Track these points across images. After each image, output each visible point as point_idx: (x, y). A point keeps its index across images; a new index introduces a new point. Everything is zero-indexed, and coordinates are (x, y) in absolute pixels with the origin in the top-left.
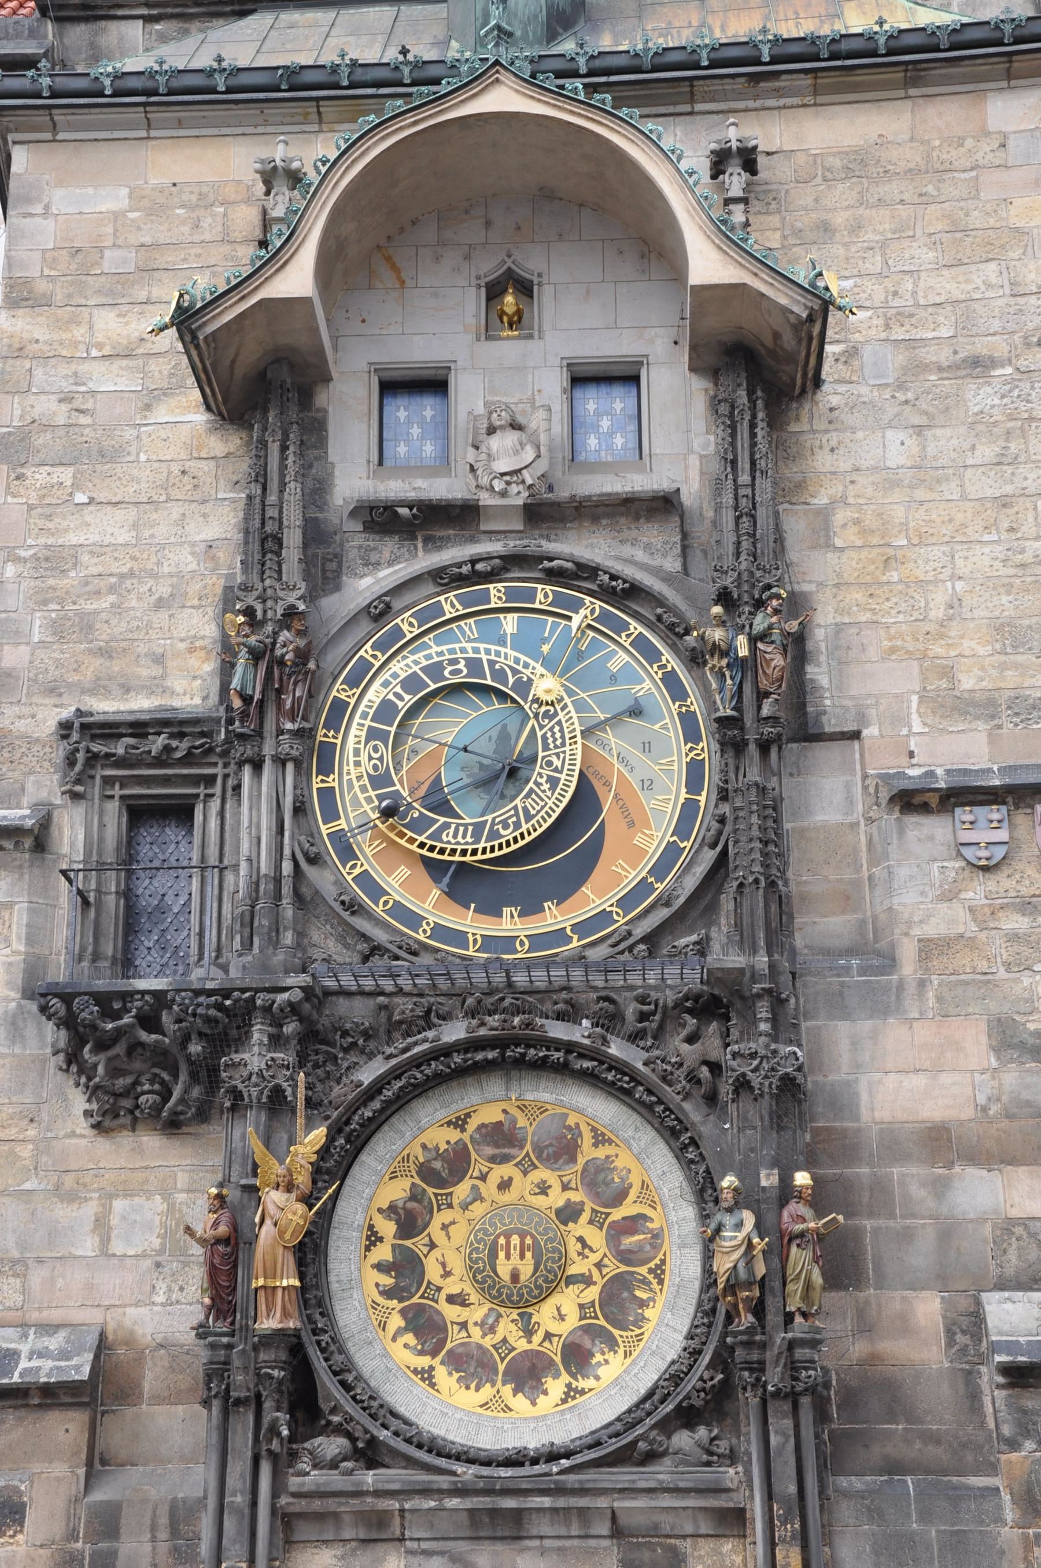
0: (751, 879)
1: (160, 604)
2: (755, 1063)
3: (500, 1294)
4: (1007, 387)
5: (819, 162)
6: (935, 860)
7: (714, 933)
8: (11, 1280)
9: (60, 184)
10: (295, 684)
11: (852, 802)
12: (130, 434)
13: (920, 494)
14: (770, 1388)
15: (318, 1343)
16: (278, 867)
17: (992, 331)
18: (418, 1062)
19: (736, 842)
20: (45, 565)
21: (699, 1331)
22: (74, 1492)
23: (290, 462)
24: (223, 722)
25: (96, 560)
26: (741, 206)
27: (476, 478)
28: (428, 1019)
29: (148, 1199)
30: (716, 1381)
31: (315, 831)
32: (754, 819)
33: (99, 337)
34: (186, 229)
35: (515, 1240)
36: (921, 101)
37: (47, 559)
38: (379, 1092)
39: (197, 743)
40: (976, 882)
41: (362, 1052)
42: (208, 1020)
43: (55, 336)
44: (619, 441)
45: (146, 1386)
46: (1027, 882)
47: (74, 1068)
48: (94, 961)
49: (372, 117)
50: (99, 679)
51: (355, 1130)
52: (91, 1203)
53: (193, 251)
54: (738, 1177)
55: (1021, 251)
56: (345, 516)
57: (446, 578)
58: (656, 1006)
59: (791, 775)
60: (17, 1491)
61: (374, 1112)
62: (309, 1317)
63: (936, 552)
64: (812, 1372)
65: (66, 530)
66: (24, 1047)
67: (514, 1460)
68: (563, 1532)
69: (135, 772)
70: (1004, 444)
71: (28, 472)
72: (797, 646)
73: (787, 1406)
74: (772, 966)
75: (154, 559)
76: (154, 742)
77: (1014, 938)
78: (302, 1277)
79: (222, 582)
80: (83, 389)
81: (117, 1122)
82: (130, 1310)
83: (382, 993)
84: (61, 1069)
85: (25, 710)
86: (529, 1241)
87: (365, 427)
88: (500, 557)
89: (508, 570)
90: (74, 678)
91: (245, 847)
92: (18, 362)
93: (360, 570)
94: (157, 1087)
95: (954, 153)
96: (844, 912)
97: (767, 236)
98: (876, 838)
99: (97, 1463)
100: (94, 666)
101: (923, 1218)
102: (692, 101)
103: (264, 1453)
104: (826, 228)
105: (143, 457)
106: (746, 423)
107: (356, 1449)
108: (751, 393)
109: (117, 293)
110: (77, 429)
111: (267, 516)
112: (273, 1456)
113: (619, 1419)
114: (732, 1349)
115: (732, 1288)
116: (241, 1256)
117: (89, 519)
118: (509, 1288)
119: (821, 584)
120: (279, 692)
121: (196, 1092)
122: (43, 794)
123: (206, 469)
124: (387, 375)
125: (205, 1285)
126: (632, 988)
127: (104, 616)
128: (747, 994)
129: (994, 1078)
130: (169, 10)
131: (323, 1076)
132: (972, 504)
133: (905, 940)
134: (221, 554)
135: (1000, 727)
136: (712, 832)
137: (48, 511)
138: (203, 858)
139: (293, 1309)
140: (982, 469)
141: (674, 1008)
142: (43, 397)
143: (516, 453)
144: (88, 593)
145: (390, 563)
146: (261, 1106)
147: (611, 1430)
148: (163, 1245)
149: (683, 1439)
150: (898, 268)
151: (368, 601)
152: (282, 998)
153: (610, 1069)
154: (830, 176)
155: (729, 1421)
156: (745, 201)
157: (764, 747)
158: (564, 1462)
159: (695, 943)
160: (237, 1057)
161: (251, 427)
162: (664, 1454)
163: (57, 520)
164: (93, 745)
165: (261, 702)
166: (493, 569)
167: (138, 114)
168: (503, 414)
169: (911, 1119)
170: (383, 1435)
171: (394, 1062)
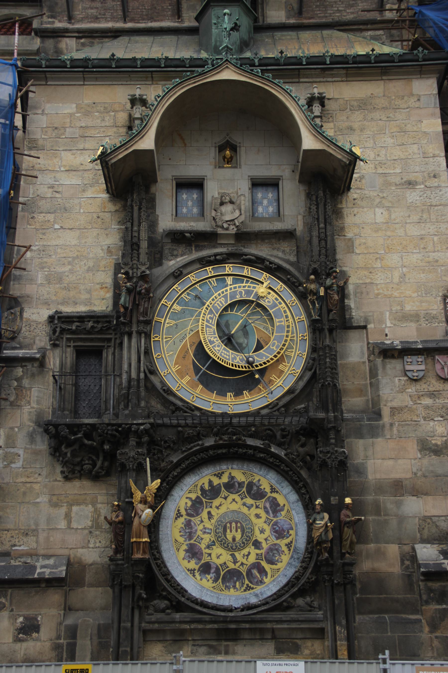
1: (89, 270)
2: (329, 455)
4: (422, 193)
5: (348, 102)
6: (396, 377)
7: (311, 404)
8: (32, 538)
9: (48, 102)
10: (145, 302)
11: (363, 353)
12: (76, 201)
14: (335, 582)
15: (157, 563)
16: (138, 375)
17: (416, 171)
19: (320, 369)
20: (42, 253)
22: (59, 621)
23: (142, 214)
25: (63, 251)
26: (319, 119)
27: (216, 222)
28: (199, 437)
29: (86, 506)
31: (152, 361)
32: (328, 360)
33: (64, 163)
34: (99, 121)
35: (234, 525)
36: (387, 81)
38: (180, 465)
41: (172, 449)
42: (113, 436)
44: (271, 209)
45: (87, 580)
46: (432, 386)
47: (57, 454)
49: (177, 80)
50: (64, 298)
52: (63, 508)
53: (102, 130)
54: (322, 500)
55: (426, 141)
57: (205, 262)
59: (339, 342)
61: (178, 473)
62: (153, 553)
64: (351, 576)
68: (253, 637)
69: (79, 336)
70: (421, 215)
72: (342, 292)
73: (342, 589)
74: (335, 417)
76: (88, 324)
77: (427, 407)
78: (150, 537)
79: (114, 261)
80: (57, 183)
82: (80, 551)
83: (180, 426)
85: (35, 311)
86: (239, 525)
87: (171, 201)
88: (226, 254)
89: (229, 259)
90: (54, 298)
91: (125, 367)
93: (170, 258)
94: (91, 462)
96: (360, 396)
97: (329, 130)
99: (68, 609)
101: (392, 516)
102: (299, 77)
104: (351, 129)
105: (82, 211)
106: (322, 204)
107: (172, 605)
108: (324, 192)
110: (55, 199)
112: (140, 608)
113: (275, 594)
115: (320, 543)
120: (138, 305)
121: (106, 464)
122: (42, 344)
123: (107, 216)
125: (113, 540)
126: (279, 425)
127: (66, 274)
130: (86, 35)
131: (157, 458)
132: (409, 238)
133: (385, 408)
134: (113, 250)
136: (310, 364)
138: (106, 371)
139: (147, 550)
140: (413, 224)
142: (42, 186)
143: (232, 213)
145: (182, 255)
146: (134, 470)
147: (271, 598)
148: (93, 524)
149: (300, 601)
150: (380, 145)
152: (142, 427)
153: (271, 457)
154: (352, 109)
156: (320, 117)
157: (331, 331)
158: (255, 611)
159: (304, 408)
160: (123, 451)
162: (293, 607)
163: (47, 235)
165: (131, 310)
166: (223, 258)
167: (81, 75)
168: (227, 197)
169: (387, 477)
170: (183, 599)
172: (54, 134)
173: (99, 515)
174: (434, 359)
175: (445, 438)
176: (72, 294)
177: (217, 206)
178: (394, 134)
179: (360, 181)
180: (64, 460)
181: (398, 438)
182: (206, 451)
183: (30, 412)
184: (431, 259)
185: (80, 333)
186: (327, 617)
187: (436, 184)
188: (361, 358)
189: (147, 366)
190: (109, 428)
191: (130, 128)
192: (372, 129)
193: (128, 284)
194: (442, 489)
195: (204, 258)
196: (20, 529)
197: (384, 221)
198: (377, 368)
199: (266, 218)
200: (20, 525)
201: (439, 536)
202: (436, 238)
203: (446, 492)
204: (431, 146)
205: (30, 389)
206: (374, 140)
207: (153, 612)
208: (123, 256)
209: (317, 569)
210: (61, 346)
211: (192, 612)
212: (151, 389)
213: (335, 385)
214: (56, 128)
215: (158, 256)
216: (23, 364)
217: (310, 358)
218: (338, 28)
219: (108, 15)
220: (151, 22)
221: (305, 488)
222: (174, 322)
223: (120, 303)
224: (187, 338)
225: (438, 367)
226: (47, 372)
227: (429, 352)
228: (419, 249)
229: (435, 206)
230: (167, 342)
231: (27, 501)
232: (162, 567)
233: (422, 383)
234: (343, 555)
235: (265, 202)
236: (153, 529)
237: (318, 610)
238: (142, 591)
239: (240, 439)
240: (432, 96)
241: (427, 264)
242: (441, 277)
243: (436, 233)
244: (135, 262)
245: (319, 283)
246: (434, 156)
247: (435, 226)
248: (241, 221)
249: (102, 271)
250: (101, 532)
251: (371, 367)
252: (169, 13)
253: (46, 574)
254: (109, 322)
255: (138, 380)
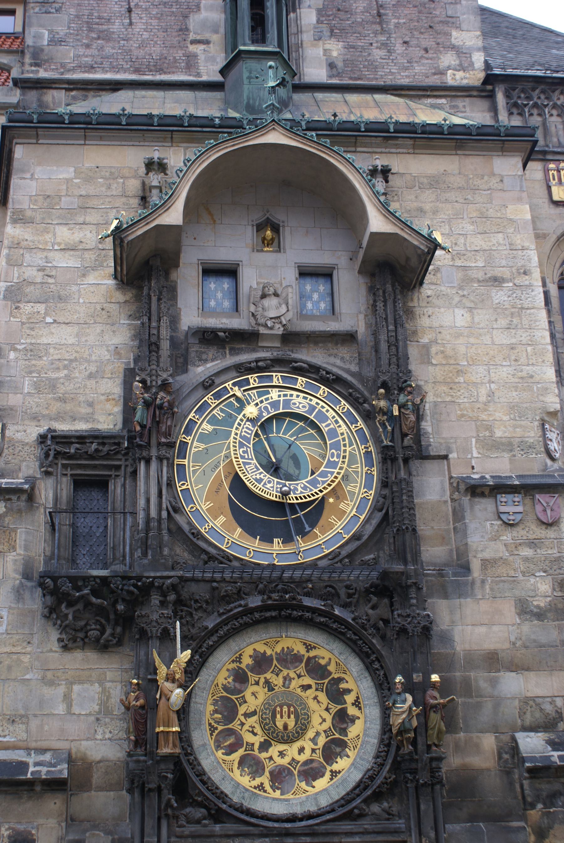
0: (404, 527)
1: (91, 376)
2: (409, 619)
3: (278, 736)
6: (488, 520)
8: (21, 726)
9: (39, 164)
10: (167, 418)
11: (444, 491)
12: (74, 288)
13: (472, 340)
14: (421, 781)
15: (188, 760)
18: (236, 617)
19: (394, 510)
21: (382, 754)
22: (60, 834)
23: (162, 306)
24: (126, 438)
25: (57, 352)
28: (240, 594)
29: (91, 685)
30: (392, 779)
31: (177, 496)
33: (58, 240)
34: (103, 189)
35: (285, 709)
36: (463, 157)
37: (31, 350)
39: (112, 448)
40: (507, 532)
41: (205, 611)
43: (36, 238)
44: (322, 305)
46: (532, 532)
48: (58, 560)
50: (59, 413)
51: (204, 651)
52: (61, 687)
53: (107, 200)
56: (189, 335)
58: (356, 590)
60: (30, 833)
61: (214, 642)
63: (481, 369)
65: (41, 336)
66: (24, 603)
67: (293, 818)
70: (510, 319)
71: (21, 306)
72: (418, 411)
75: (87, 352)
76: (90, 447)
77: (526, 559)
78: (180, 726)
79: (123, 366)
80: (50, 265)
81: (75, 645)
82: (83, 743)
84: (45, 616)
85: (21, 428)
86: (292, 709)
88: (270, 360)
89: (273, 366)
90: (45, 412)
91: (142, 502)
92: (16, 250)
94: (98, 627)
95: (479, 182)
96: (442, 545)
98: (458, 508)
99: (71, 821)
100: (56, 407)
101: (486, 697)
102: (355, 146)
103: (163, 815)
104: (421, 210)
105: (81, 301)
107: (209, 813)
108: (393, 286)
109: (68, 218)
110: (47, 285)
111: (151, 333)
113: (342, 798)
114: (400, 763)
115: (400, 732)
116: (149, 715)
117: (53, 331)
118: (282, 733)
119: (426, 381)
120: (158, 423)
121: (119, 629)
122: (31, 472)
124: (206, 266)
125: (131, 730)
127: (61, 380)
128: (404, 585)
129: (518, 628)
130: (79, 86)
132: (497, 347)
133: (475, 560)
134: (122, 352)
135: (514, 456)
136: (380, 503)
137: (32, 325)
138: (114, 508)
139: (178, 742)
140: (501, 330)
141: (365, 592)
142: (29, 268)
143: (277, 308)
144: (53, 369)
145: (213, 360)
146: (157, 637)
147: (339, 804)
149: (375, 808)
151: (203, 379)
153: (334, 622)
154: (422, 186)
155: (396, 798)
159: (374, 559)
161: (140, 288)
164: (57, 448)
168: (271, 288)
170: (224, 806)
171: (224, 617)
172: (45, 204)
173: (109, 697)
174: (533, 499)
175: (549, 599)
176: (68, 407)
177: (256, 299)
178: (474, 219)
179: (434, 275)
180: (64, 624)
181: (491, 599)
182: (251, 614)
183: (16, 560)
184: (524, 374)
185: (80, 457)
186: (410, 827)
187: (527, 283)
188: (442, 496)
189: (170, 502)
190: (124, 582)
191: (144, 199)
192: (447, 213)
193: (146, 395)
194: (547, 663)
195: (242, 364)
196: (4, 714)
197: (466, 326)
198: (463, 509)
199: (317, 316)
200: (5, 709)
201: (544, 722)
202: (529, 349)
203: (551, 666)
204: (518, 237)
205: (15, 530)
206: (449, 225)
207: (185, 824)
208: (137, 360)
209: (396, 766)
210: (55, 474)
211: (235, 823)
212: (177, 532)
213: (414, 530)
214: (48, 196)
215: (181, 360)
216: (7, 497)
217: (381, 495)
218: (392, 92)
219: (106, 65)
220: (160, 74)
221: (379, 662)
222: (203, 446)
223: (136, 419)
224: (221, 467)
225: (539, 508)
226: (38, 507)
227: (528, 489)
228: (510, 361)
229: (527, 309)
230: (194, 472)
231: (13, 677)
232: (195, 765)
233: (519, 529)
234: (429, 747)
235: (315, 296)
236: (182, 716)
237: (397, 818)
238: (171, 796)
239: (294, 599)
240: (517, 177)
241: (521, 381)
242: (537, 397)
243: (530, 343)
244: (154, 367)
245: (389, 400)
246: (523, 249)
247: (528, 334)
248: (288, 319)
249: (108, 378)
250: (112, 719)
251: (455, 507)
252: (183, 64)
253: (43, 773)
254: (118, 444)
255: (160, 520)
